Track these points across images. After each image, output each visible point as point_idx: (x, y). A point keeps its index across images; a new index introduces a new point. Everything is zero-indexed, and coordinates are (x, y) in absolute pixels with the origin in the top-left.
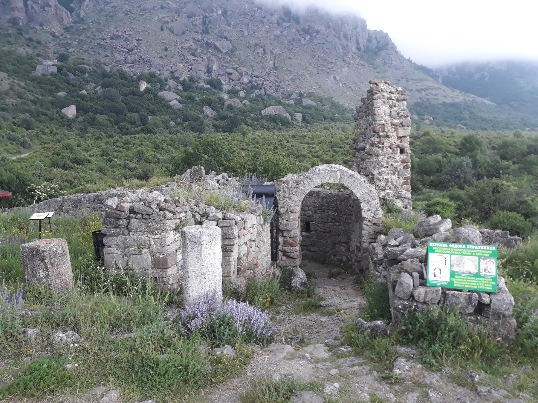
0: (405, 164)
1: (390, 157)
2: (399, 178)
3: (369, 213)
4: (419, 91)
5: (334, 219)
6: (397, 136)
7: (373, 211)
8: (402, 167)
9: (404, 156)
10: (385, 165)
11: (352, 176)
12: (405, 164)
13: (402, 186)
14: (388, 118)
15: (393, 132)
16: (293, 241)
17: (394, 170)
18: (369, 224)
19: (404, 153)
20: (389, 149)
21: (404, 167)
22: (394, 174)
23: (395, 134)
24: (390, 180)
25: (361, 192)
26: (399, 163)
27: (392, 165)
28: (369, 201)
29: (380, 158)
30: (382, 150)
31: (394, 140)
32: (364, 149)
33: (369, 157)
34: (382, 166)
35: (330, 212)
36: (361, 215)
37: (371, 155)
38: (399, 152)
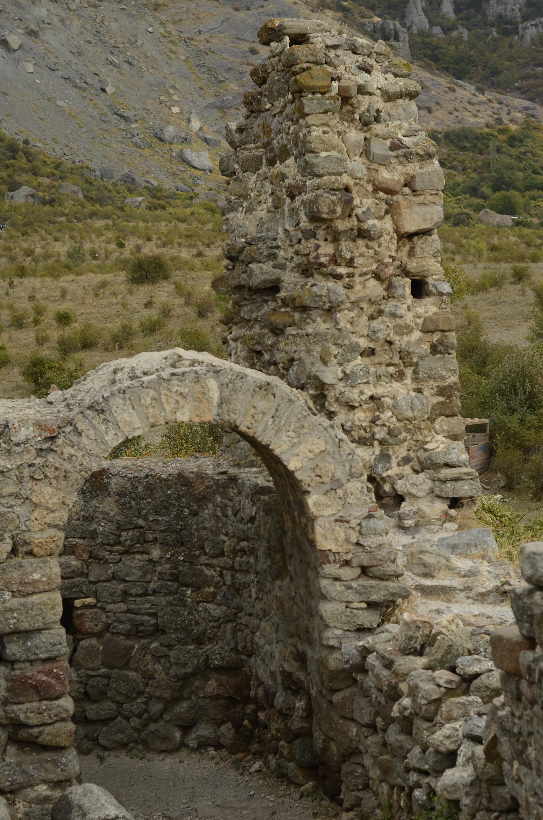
0: (436, 337)
1: (381, 312)
2: (419, 391)
3: (341, 532)
5: (175, 578)
6: (396, 231)
7: (354, 523)
8: (426, 347)
9: (428, 307)
10: (364, 343)
11: (265, 388)
12: (436, 337)
13: (432, 420)
14: (358, 164)
15: (380, 218)
16: (49, 673)
17: (396, 360)
18: (347, 573)
19: (428, 294)
20: (373, 283)
21: (434, 349)
22: (400, 376)
23: (388, 224)
24: (388, 401)
25: (303, 448)
26: (417, 335)
27: (390, 343)
28: (337, 484)
29: (343, 317)
30: (349, 287)
31: (388, 247)
32: (273, 288)
33: (297, 316)
34: (353, 348)
35: (156, 553)
36: (312, 543)
37: (304, 309)
38: (408, 291)
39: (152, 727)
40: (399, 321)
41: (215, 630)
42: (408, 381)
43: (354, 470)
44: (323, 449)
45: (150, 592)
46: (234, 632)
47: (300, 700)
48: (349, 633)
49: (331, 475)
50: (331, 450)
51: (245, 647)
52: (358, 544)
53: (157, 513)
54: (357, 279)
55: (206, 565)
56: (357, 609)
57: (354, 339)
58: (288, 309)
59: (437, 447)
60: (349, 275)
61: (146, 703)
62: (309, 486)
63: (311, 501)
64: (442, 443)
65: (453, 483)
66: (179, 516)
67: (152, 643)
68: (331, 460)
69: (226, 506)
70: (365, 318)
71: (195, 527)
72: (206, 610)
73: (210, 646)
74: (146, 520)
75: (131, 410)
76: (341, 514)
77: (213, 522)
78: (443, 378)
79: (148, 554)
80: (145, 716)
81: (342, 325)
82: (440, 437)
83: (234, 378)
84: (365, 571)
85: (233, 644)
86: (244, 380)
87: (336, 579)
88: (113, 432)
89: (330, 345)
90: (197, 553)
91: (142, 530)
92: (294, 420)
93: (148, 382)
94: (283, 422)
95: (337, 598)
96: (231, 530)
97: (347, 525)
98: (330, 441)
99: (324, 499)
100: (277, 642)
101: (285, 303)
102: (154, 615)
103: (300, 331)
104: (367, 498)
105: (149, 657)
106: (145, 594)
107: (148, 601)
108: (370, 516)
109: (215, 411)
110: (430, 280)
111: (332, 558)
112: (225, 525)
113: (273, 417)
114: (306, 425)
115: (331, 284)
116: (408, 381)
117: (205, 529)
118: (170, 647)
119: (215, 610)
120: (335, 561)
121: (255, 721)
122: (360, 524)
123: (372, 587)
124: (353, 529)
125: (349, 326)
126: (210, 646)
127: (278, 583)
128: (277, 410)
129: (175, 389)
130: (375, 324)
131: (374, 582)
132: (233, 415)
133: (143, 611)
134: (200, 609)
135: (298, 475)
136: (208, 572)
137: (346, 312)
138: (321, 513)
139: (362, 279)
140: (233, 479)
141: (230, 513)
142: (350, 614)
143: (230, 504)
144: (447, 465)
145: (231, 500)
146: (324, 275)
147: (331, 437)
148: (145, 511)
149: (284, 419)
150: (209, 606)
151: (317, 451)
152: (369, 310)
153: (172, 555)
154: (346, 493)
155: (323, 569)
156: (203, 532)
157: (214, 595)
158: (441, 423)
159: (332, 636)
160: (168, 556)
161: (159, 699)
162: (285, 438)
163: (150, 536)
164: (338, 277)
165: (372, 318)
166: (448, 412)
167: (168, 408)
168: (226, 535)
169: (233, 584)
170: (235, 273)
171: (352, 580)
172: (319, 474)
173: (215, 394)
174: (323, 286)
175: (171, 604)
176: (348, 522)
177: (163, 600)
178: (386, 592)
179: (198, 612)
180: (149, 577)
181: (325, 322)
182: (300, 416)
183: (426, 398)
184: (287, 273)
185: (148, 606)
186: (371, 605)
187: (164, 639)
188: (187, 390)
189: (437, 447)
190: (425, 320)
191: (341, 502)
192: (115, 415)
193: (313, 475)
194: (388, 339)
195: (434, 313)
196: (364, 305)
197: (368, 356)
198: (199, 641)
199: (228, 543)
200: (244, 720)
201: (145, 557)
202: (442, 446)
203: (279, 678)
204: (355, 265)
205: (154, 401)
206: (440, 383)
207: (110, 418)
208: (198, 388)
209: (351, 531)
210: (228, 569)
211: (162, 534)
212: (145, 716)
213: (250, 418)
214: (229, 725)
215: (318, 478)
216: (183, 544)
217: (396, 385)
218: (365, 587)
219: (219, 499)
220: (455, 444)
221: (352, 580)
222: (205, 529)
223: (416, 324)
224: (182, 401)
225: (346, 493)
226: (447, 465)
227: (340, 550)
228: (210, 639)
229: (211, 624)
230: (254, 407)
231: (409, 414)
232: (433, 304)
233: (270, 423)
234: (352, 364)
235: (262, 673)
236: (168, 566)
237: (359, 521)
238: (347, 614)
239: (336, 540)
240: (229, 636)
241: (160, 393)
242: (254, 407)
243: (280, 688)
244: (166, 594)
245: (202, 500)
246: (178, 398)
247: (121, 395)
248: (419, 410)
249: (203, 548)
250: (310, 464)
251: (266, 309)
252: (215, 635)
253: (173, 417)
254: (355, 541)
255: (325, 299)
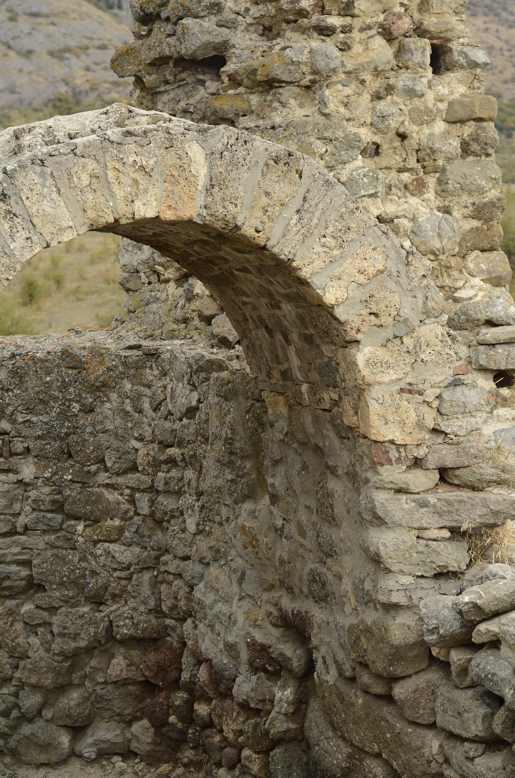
1: (390, 89)
2: (447, 211)
3: (410, 409)
4: (58, 55)
5: (58, 507)
7: (430, 394)
9: (453, 87)
10: (366, 135)
12: (468, 129)
17: (412, 163)
18: (422, 480)
20: (379, 42)
21: (466, 149)
22: (418, 188)
25: (349, 267)
26: (440, 126)
27: (403, 137)
29: (333, 96)
32: (213, 61)
33: (255, 99)
34: (351, 143)
35: (28, 470)
37: (270, 85)
39: (26, 729)
40: (416, 102)
41: (124, 582)
42: (430, 195)
43: (431, 304)
44: (381, 268)
45: (19, 530)
46: (155, 584)
47: (284, 687)
48: (423, 581)
49: (394, 313)
50: (394, 269)
51: (174, 607)
52: (435, 431)
53: (30, 410)
54: (356, 35)
55: (107, 486)
56: (434, 540)
57: (351, 128)
58: (242, 89)
59: (476, 295)
60: (346, 30)
61: (16, 695)
62: (359, 331)
63: (362, 356)
64: (480, 289)
65: (506, 347)
66: (64, 415)
67: (22, 604)
68: (394, 287)
69: (140, 396)
70: (366, 97)
71: (89, 429)
72: (108, 553)
73: (115, 607)
74: (13, 421)
75: (55, 196)
76: (409, 380)
77: (118, 421)
78: (481, 191)
79: (16, 472)
80: (15, 713)
81: (332, 107)
82: (477, 281)
83: (232, 142)
84: (445, 475)
85: (152, 603)
86: (249, 145)
87: (399, 491)
88: (24, 234)
89: (312, 139)
90: (93, 468)
91: (6, 438)
92: (333, 216)
93: (85, 146)
94: (315, 221)
95: (404, 523)
96: (148, 432)
97: (420, 399)
98: (393, 254)
99: (382, 354)
100: (241, 599)
101: (235, 81)
102: (27, 564)
103: (261, 122)
104: (451, 352)
105: (19, 626)
106: (13, 532)
107: (17, 544)
108: (456, 383)
109: (200, 200)
110: (455, 46)
111: (393, 454)
112: (138, 424)
113: (298, 211)
114: (353, 225)
115: (315, 43)
116: (430, 195)
117: (105, 431)
118: (52, 610)
119: (123, 554)
120: (399, 460)
121: (188, 716)
122: (439, 397)
123: (461, 502)
124: (428, 404)
125: (342, 109)
126: (115, 607)
127: (248, 506)
128: (305, 199)
129: (131, 159)
130: (382, 106)
131: (464, 494)
132: (231, 207)
133: (9, 558)
134: (99, 552)
135: (340, 313)
136: (112, 496)
137: (339, 87)
138: (378, 378)
139: (364, 36)
140: (153, 355)
141: (146, 405)
142: (425, 550)
143: (148, 392)
144: (490, 323)
145: (149, 386)
146: (303, 30)
147: (394, 246)
148: (11, 409)
149: (317, 214)
150: (113, 547)
151: (371, 271)
152: (374, 84)
153: (54, 474)
154: (418, 345)
155: (377, 473)
156: (103, 438)
157: (121, 530)
158: (475, 261)
159: (395, 586)
160: (47, 475)
161: (35, 687)
162: (318, 248)
163: (19, 446)
164: (325, 31)
165: (377, 97)
166: (486, 244)
167: (120, 193)
168: (141, 439)
169: (152, 515)
170: (152, 40)
171: (426, 491)
172: (374, 310)
173: (201, 170)
174: (300, 48)
175: (53, 546)
176: (421, 393)
177: (38, 541)
178: (484, 510)
179: (95, 557)
180: (17, 507)
181: (301, 106)
182: (343, 210)
183: (457, 221)
184: (239, 34)
185: (16, 550)
186: (456, 533)
187: (41, 598)
188: (152, 162)
189: (476, 295)
190: (451, 104)
191: (409, 359)
192: (27, 203)
193: (365, 312)
194: (402, 130)
195: (462, 95)
196: (367, 77)
197: (371, 156)
198: (97, 601)
199: (144, 453)
200: (169, 715)
201: (12, 477)
202: (481, 294)
203: (244, 655)
204: (356, 12)
205: (94, 181)
206: (476, 199)
207: (17, 209)
208: (171, 158)
209: (425, 409)
210: (143, 491)
211: (38, 442)
212: (15, 713)
213: (260, 213)
214: (145, 722)
215: (373, 317)
216: (70, 456)
217: (414, 201)
218: (449, 503)
219: (129, 386)
220: (498, 291)
221: (426, 491)
222: (105, 431)
223: (439, 111)
224: (143, 182)
225: (418, 345)
226: (490, 323)
227: (408, 440)
228: (115, 597)
229: (117, 574)
230: (267, 194)
231: (436, 244)
232: (460, 82)
233: (294, 221)
234: (349, 167)
235: (209, 646)
236: (47, 490)
237: (438, 391)
238: (420, 549)
239: (402, 423)
240: (146, 590)
241: (106, 167)
242: (267, 194)
243: (244, 669)
244: (44, 532)
245: (101, 388)
246: (136, 176)
247: (38, 169)
248: (450, 238)
249: (103, 461)
250: (359, 294)
251: (202, 93)
252: (124, 591)
253: (129, 209)
254: (431, 426)
255: (304, 69)
